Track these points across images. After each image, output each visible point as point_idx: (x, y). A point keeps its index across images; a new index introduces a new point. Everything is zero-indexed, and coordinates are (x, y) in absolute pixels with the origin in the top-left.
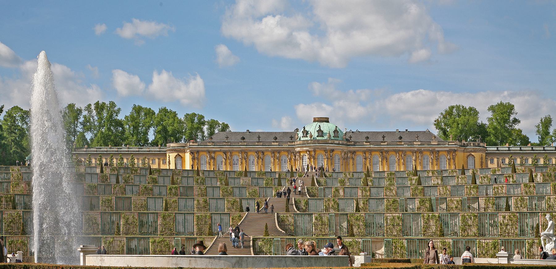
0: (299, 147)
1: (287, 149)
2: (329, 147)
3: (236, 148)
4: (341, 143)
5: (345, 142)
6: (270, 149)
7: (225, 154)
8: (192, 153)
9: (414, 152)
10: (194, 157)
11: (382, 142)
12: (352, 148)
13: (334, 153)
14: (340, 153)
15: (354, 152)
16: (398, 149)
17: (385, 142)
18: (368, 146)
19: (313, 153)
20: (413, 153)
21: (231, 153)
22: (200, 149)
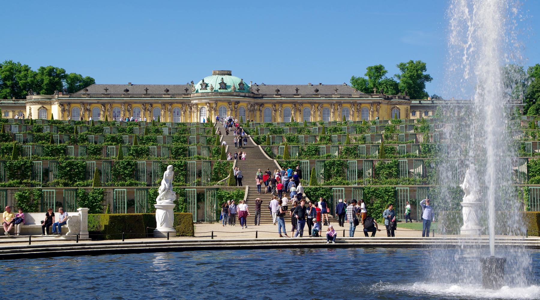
4: (247, 95)
5: (252, 95)
7: (104, 106)
8: (61, 104)
9: (331, 104)
10: (64, 109)
11: (295, 95)
12: (260, 101)
13: (239, 105)
15: (262, 105)
16: (314, 101)
17: (298, 95)
18: (279, 98)
19: (214, 106)
20: (331, 105)
21: (111, 104)
22: (72, 101)
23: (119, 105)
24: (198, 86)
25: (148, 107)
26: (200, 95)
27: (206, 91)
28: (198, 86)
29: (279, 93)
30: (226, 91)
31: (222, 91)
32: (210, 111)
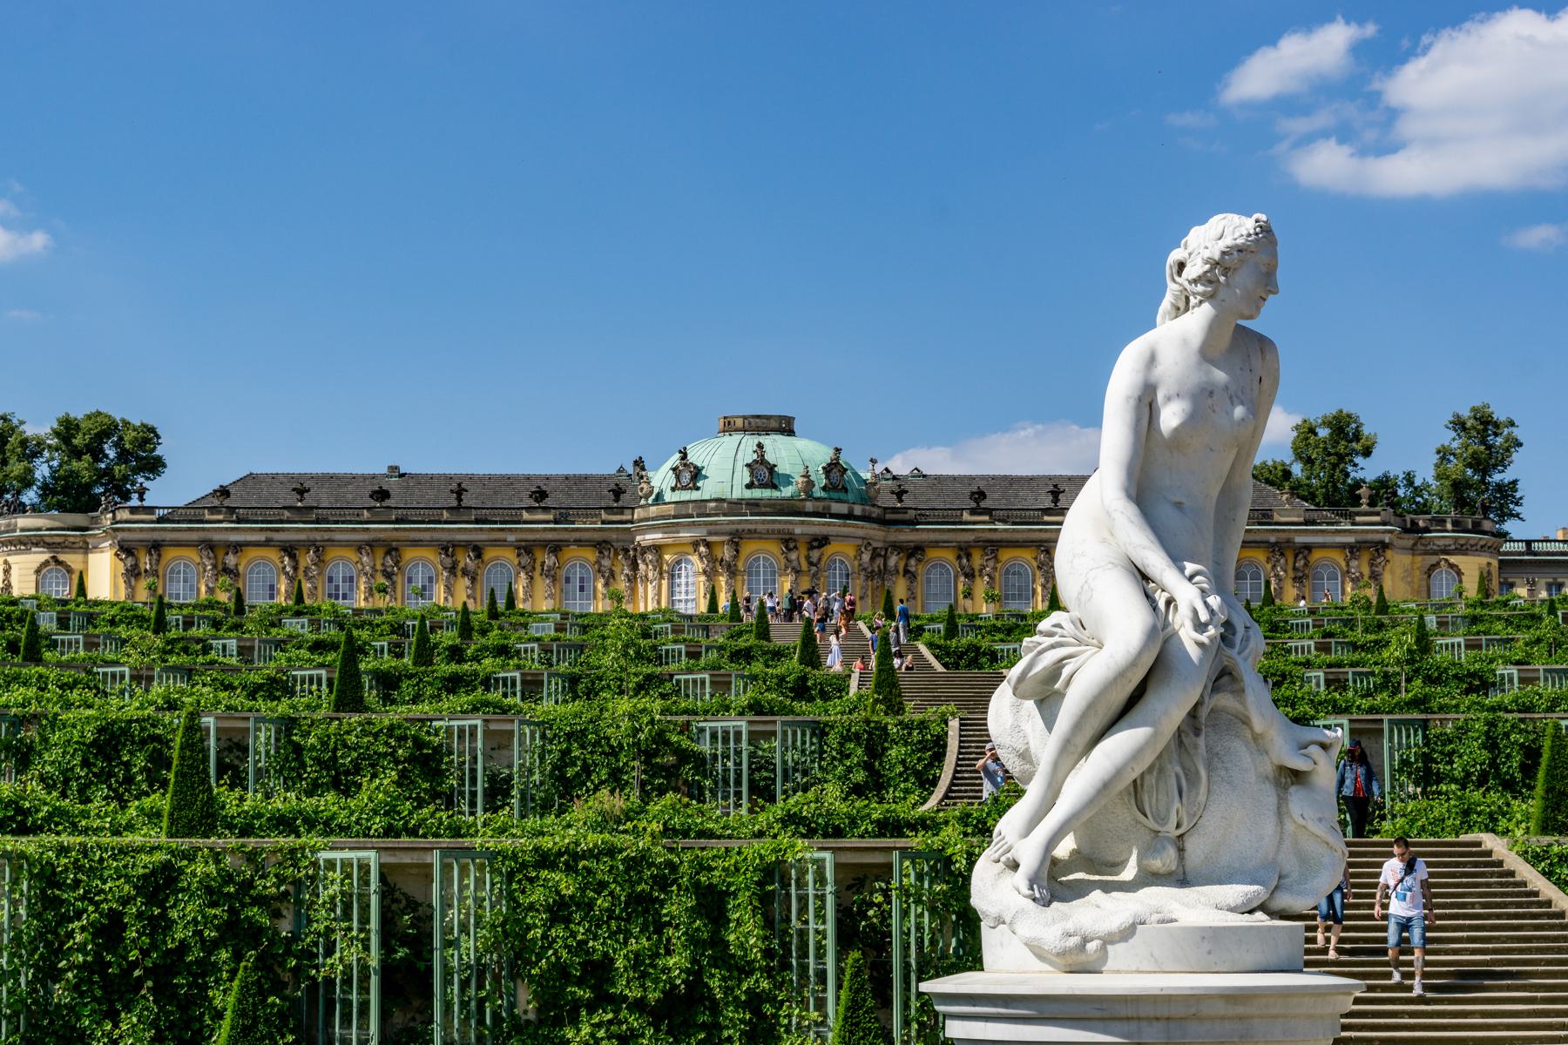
0: (654, 528)
1: (597, 536)
2: (801, 527)
3: (343, 531)
4: (858, 510)
6: (511, 538)
7: (293, 557)
8: (126, 549)
11: (1047, 511)
12: (906, 536)
13: (829, 550)
14: (852, 552)
18: (983, 526)
19: (726, 553)
21: (319, 548)
22: (169, 536)
23: (351, 555)
24: (661, 478)
25: (465, 560)
26: (671, 510)
27: (695, 495)
28: (661, 478)
29: (983, 504)
30: (776, 494)
31: (757, 493)
32: (710, 574)
